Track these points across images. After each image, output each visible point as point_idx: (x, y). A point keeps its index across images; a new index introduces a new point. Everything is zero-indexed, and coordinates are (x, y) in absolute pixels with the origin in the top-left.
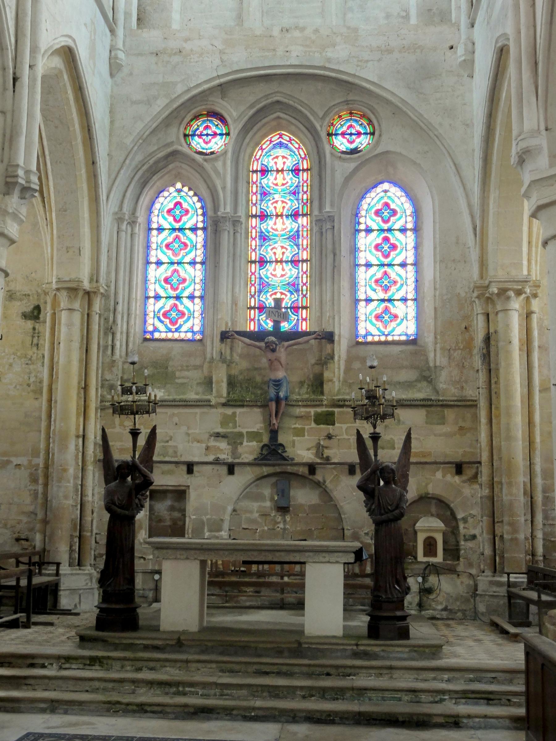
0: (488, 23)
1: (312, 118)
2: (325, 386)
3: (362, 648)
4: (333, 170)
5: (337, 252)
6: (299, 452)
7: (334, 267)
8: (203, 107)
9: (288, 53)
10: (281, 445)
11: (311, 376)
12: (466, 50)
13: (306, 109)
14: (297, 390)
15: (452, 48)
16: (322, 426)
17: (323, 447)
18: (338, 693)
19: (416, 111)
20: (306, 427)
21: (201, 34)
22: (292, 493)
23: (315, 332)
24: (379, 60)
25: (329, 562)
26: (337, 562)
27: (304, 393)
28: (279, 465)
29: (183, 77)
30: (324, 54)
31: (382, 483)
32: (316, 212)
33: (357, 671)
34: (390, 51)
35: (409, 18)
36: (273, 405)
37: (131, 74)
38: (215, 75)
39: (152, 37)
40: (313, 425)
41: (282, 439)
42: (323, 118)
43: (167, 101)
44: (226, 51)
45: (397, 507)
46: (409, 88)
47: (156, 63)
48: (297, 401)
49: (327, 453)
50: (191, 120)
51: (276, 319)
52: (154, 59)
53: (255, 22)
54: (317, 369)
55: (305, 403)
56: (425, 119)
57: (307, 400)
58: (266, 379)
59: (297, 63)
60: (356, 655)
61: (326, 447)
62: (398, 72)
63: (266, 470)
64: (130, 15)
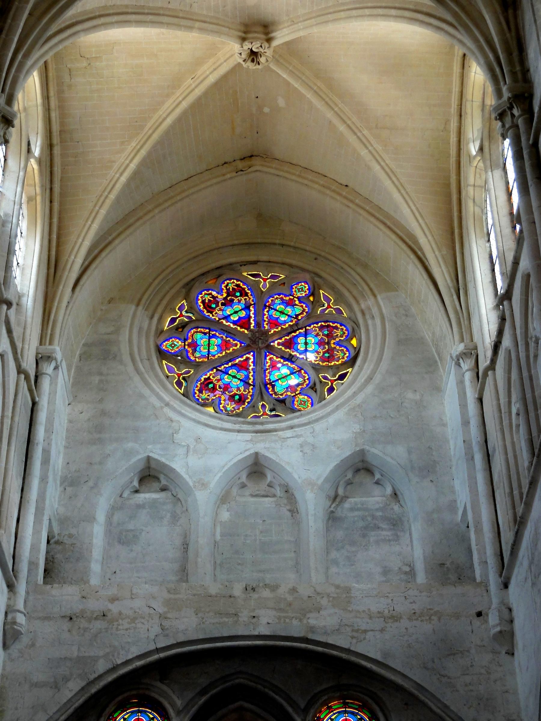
0: (533, 584)
1: (290, 710)
8: (134, 692)
9: (254, 620)
12: (501, 619)
13: (280, 696)
15: (479, 614)
19: (439, 700)
21: (134, 591)
24: (382, 630)
29: (107, 650)
30: (305, 621)
34: (395, 618)
37: (33, 645)
38: (152, 647)
39: (66, 595)
42: (305, 711)
43: (83, 683)
44: (169, 615)
46: (426, 668)
47: (69, 631)
50: (115, 711)
52: (66, 625)
53: (206, 577)
56: (453, 712)
59: (268, 633)
62: (409, 646)
64: (37, 565)
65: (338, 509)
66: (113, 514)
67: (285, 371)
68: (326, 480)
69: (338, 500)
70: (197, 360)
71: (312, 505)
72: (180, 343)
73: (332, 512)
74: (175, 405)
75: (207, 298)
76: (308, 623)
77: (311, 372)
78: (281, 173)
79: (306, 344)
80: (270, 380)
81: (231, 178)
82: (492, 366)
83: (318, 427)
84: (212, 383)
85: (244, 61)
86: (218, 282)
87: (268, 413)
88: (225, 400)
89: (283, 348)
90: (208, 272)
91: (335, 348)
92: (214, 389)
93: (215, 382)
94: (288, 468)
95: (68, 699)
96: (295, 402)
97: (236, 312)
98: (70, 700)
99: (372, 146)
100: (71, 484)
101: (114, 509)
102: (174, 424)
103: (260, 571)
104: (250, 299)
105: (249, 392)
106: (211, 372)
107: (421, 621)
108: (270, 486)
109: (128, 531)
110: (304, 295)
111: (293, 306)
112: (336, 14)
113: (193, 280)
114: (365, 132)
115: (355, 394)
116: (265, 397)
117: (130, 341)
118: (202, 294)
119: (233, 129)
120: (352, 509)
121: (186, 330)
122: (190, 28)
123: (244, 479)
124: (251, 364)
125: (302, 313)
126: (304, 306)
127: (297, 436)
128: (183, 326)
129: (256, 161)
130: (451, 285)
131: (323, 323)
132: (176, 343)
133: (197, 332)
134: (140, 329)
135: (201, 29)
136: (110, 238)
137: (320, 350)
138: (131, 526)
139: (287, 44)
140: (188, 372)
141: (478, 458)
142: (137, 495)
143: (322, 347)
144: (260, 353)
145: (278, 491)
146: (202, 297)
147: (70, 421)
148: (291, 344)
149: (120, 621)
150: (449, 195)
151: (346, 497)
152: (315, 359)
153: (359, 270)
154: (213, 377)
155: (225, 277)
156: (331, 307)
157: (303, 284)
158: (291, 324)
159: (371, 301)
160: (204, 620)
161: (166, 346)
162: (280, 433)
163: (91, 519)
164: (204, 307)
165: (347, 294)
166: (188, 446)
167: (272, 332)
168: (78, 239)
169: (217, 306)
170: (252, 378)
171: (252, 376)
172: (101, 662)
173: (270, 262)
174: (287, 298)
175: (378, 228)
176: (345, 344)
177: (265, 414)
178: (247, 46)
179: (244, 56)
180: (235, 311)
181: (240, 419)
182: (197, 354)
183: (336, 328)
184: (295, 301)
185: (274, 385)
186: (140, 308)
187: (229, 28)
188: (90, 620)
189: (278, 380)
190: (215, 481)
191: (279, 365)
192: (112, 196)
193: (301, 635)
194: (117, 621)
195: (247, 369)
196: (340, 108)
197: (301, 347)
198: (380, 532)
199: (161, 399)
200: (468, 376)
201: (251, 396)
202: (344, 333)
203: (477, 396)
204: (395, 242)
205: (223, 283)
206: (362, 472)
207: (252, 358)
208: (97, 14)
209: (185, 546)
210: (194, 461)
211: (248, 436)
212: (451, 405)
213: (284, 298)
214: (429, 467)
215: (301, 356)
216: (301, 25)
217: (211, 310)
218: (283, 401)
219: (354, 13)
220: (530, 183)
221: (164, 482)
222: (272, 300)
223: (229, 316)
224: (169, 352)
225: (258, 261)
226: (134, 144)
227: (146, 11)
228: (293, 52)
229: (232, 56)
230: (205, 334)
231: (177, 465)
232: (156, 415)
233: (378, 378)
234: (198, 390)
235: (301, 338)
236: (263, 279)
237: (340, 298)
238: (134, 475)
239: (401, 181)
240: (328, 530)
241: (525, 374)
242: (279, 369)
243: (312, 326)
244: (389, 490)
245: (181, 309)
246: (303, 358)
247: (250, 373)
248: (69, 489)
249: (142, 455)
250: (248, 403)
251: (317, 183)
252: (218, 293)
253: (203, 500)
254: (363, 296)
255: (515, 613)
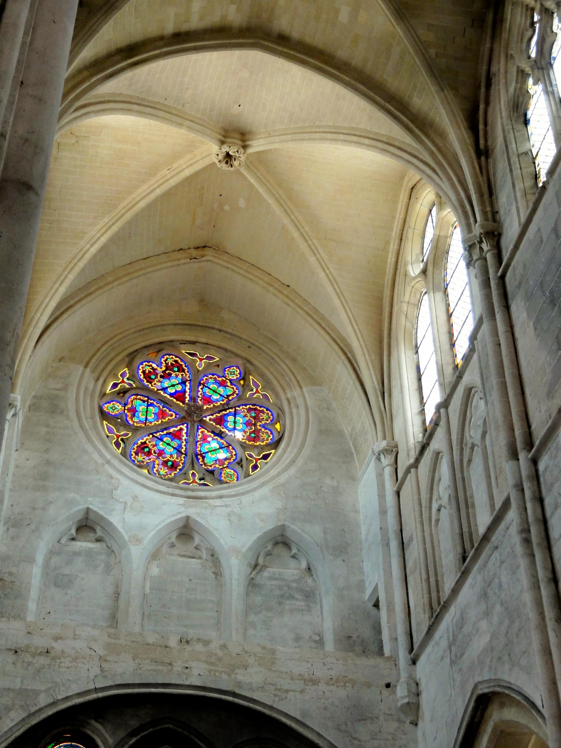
0: (452, 663)
9: (187, 671)
12: (409, 691)
15: (388, 686)
21: (77, 633)
24: (302, 692)
29: (49, 685)
30: (233, 676)
34: (315, 682)
35: (323, 644)
38: (91, 686)
43: (25, 715)
44: (109, 658)
46: (340, 731)
47: (14, 663)
52: (11, 658)
59: (199, 684)
62: (325, 708)
65: (258, 576)
66: (50, 558)
67: (214, 445)
68: (250, 549)
69: (258, 568)
70: (135, 424)
71: (235, 569)
72: (120, 407)
73: (253, 579)
74: (115, 464)
75: (148, 369)
76: (237, 679)
77: (239, 449)
78: (230, 266)
79: (235, 422)
80: (200, 451)
81: (184, 264)
82: (416, 465)
83: (245, 499)
84: (147, 447)
85: (219, 162)
86: (158, 356)
87: (198, 481)
88: (158, 465)
89: (214, 424)
90: (151, 345)
91: (261, 430)
92: (149, 453)
93: (151, 447)
94: (217, 534)
95: (9, 728)
96: (223, 475)
97: (173, 386)
98: (11, 729)
99: (320, 254)
100: (14, 526)
101: (52, 553)
102: (114, 481)
103: (185, 626)
104: (186, 375)
105: (181, 460)
106: (147, 437)
107: (337, 686)
108: (196, 548)
109: (64, 575)
110: (235, 378)
111: (225, 387)
112: (311, 134)
113: (137, 350)
114: (315, 241)
115: (279, 474)
116: (196, 466)
117: (77, 399)
118: (142, 365)
119: (194, 219)
120: (270, 578)
121: (127, 395)
122: (180, 125)
123: (173, 539)
124: (184, 434)
125: (232, 394)
126: (235, 388)
127: (226, 506)
128: (124, 392)
129: (207, 251)
130: (377, 387)
131: (251, 406)
132: (116, 406)
133: (136, 399)
134: (86, 389)
135: (189, 128)
136: (72, 302)
137: (247, 430)
138: (66, 571)
139: (258, 153)
140: (126, 435)
141: (394, 545)
142: (73, 542)
143: (249, 427)
144: (193, 425)
145: (204, 555)
146: (143, 368)
147: (17, 467)
148: (221, 421)
149: (62, 659)
150: (380, 308)
151: (264, 567)
152: (242, 437)
153: (288, 362)
154: (149, 442)
155: (165, 352)
156: (259, 393)
157: (235, 368)
158: (223, 403)
159: (296, 392)
160: (141, 666)
161: (107, 408)
162: (210, 501)
163: (31, 560)
164: (145, 377)
165: (275, 383)
166: (126, 503)
167: (205, 408)
168: (44, 299)
169: (156, 377)
170: (184, 447)
171: (185, 445)
172: (42, 696)
173: (207, 344)
174: (220, 379)
175: (314, 328)
176: (269, 427)
177: (194, 481)
178: (225, 149)
179: (220, 157)
180: (172, 384)
181: (173, 484)
182: (136, 419)
183: (263, 412)
184: (227, 382)
185: (205, 457)
186: (88, 370)
187: (212, 131)
188: (33, 656)
189: (207, 452)
190: (149, 538)
191: (209, 439)
192: (81, 265)
193: (229, 688)
194: (60, 659)
195: (180, 439)
196: (296, 217)
197: (230, 425)
198: (294, 602)
199: (102, 455)
200: (388, 471)
201: (183, 464)
202: (270, 418)
203: (395, 489)
204: (328, 342)
205: (163, 357)
206: (280, 545)
207: (186, 429)
208: (107, 99)
209: (117, 596)
210: (131, 518)
211: (181, 500)
212: (367, 493)
213: (218, 379)
214: (342, 546)
215: (230, 434)
216: (277, 139)
217: (150, 381)
218: (212, 472)
219: (329, 136)
220: (496, 310)
221: (99, 533)
222: (206, 379)
223: (167, 388)
224: (110, 414)
225: (197, 342)
226: (106, 220)
227: (146, 104)
228: (261, 161)
229: (209, 155)
230: (144, 401)
231: (115, 519)
232: (97, 471)
233: (300, 462)
234: (135, 453)
235: (231, 417)
236: (200, 359)
237: (268, 385)
238: (73, 523)
239: (342, 289)
240: (247, 594)
241: (458, 475)
242: (209, 442)
243: (241, 407)
244: (304, 565)
245: (123, 375)
246: (232, 435)
247: (183, 442)
248: (12, 530)
249: (83, 506)
250: (180, 470)
251: (262, 280)
252: (158, 366)
253: (137, 554)
254: (290, 387)
255: (422, 687)
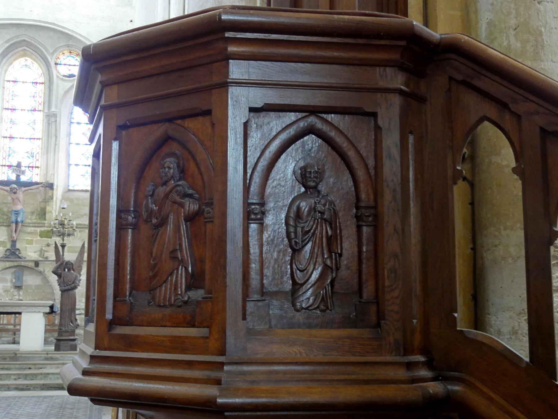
1: (45, 53)
2: (47, 215)
3: (50, 355)
4: (58, 86)
5: (58, 136)
6: (29, 254)
7: (56, 144)
10: (18, 249)
11: (39, 209)
14: (29, 217)
16: (44, 239)
17: (44, 251)
18: (35, 376)
20: (34, 239)
22: (24, 278)
23: (42, 183)
25: (35, 312)
26: (39, 312)
27: (34, 219)
28: (16, 261)
31: (66, 270)
32: (46, 111)
33: (45, 366)
36: (14, 226)
40: (39, 238)
41: (18, 246)
42: (53, 54)
45: (73, 283)
48: (29, 223)
49: (46, 254)
51: (18, 174)
54: (43, 205)
55: (34, 225)
57: (35, 223)
58: (10, 210)
60: (46, 359)
61: (46, 251)
63: (8, 264)
193: (52, 22)
